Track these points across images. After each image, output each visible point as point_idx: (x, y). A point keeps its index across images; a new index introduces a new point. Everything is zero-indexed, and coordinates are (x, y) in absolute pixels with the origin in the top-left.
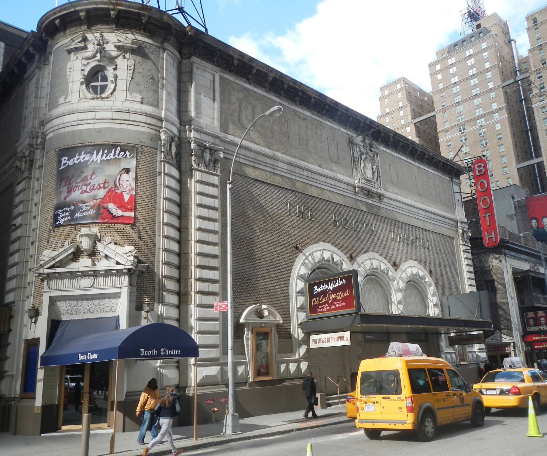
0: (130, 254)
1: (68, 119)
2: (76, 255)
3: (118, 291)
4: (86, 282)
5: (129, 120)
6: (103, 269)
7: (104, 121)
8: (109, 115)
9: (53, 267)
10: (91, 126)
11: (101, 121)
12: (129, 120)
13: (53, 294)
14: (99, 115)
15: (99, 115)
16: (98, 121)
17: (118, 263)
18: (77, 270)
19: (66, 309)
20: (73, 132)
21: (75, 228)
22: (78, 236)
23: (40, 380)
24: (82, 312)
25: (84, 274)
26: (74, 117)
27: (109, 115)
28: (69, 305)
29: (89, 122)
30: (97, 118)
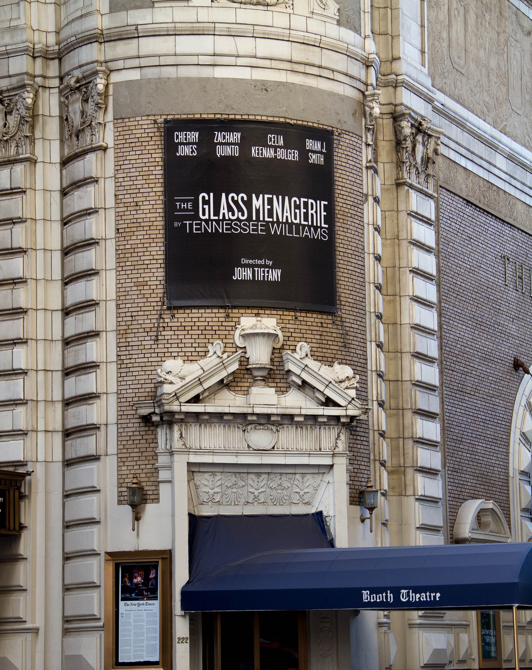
0: (346, 384)
1: (186, 44)
2: (242, 377)
3: (327, 461)
4: (261, 438)
5: (320, 67)
6: (304, 412)
7: (274, 64)
8: (282, 49)
9: (196, 399)
10: (245, 74)
11: (267, 63)
12: (320, 67)
13: (193, 459)
14: (265, 48)
15: (265, 48)
16: (261, 63)
17: (329, 402)
18: (250, 411)
19: (211, 492)
20: (204, 82)
21: (228, 316)
22: (237, 333)
23: (182, 640)
24: (243, 500)
25: (265, 420)
26: (203, 44)
27: (282, 49)
28: (219, 483)
29: (240, 61)
30: (258, 55)
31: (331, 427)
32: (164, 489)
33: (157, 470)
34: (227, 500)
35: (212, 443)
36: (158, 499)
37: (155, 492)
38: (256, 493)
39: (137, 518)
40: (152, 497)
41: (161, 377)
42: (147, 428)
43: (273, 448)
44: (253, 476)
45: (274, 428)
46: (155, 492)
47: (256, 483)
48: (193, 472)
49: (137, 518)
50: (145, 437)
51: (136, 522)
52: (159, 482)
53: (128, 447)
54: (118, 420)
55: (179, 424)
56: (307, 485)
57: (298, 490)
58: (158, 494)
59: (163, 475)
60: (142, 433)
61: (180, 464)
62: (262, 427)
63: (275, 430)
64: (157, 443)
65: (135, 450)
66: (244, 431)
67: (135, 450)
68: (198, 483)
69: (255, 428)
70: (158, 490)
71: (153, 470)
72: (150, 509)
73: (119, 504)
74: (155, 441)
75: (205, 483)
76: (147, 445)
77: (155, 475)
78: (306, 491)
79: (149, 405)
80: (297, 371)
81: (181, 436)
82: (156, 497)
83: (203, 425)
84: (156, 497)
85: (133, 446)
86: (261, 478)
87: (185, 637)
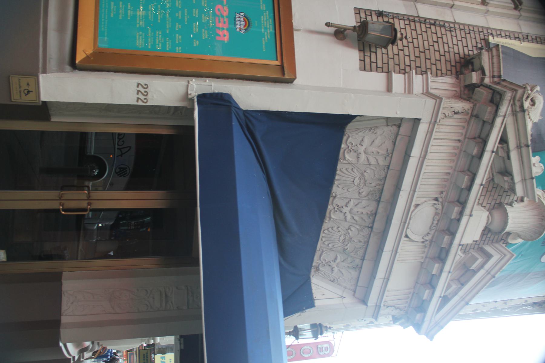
13: (422, 129)
19: (362, 149)
23: (143, 90)
28: (373, 161)
31: (409, 300)
32: (377, 79)
33: (403, 71)
34: (344, 170)
35: (434, 156)
36: (365, 70)
37: (374, 65)
38: (346, 210)
39: (340, 34)
40: (367, 59)
41: (532, 90)
42: (453, 64)
43: (407, 236)
44: (372, 207)
45: (428, 238)
46: (374, 65)
47: (361, 210)
48: (399, 126)
49: (340, 34)
50: (442, 58)
51: (332, 30)
52: (388, 72)
53: (429, 33)
54: (459, 24)
55: (470, 112)
56: (343, 271)
57: (338, 260)
58: (371, 70)
59: (398, 79)
60: (447, 54)
61: (415, 107)
62: (435, 222)
63: (425, 238)
64: (437, 76)
65: (426, 43)
66: (436, 199)
67: (426, 43)
68: (379, 131)
69: (436, 214)
70: (377, 71)
71: (402, 67)
72: (351, 56)
73: (355, 9)
74: (439, 73)
75: (377, 142)
76: (433, 61)
77: (397, 68)
78: (336, 269)
79: (495, 69)
80: (488, 266)
81: (456, 113)
82: (368, 67)
83: (459, 144)
84: (368, 67)
85: (430, 40)
86: (365, 218)
87: (149, 97)
